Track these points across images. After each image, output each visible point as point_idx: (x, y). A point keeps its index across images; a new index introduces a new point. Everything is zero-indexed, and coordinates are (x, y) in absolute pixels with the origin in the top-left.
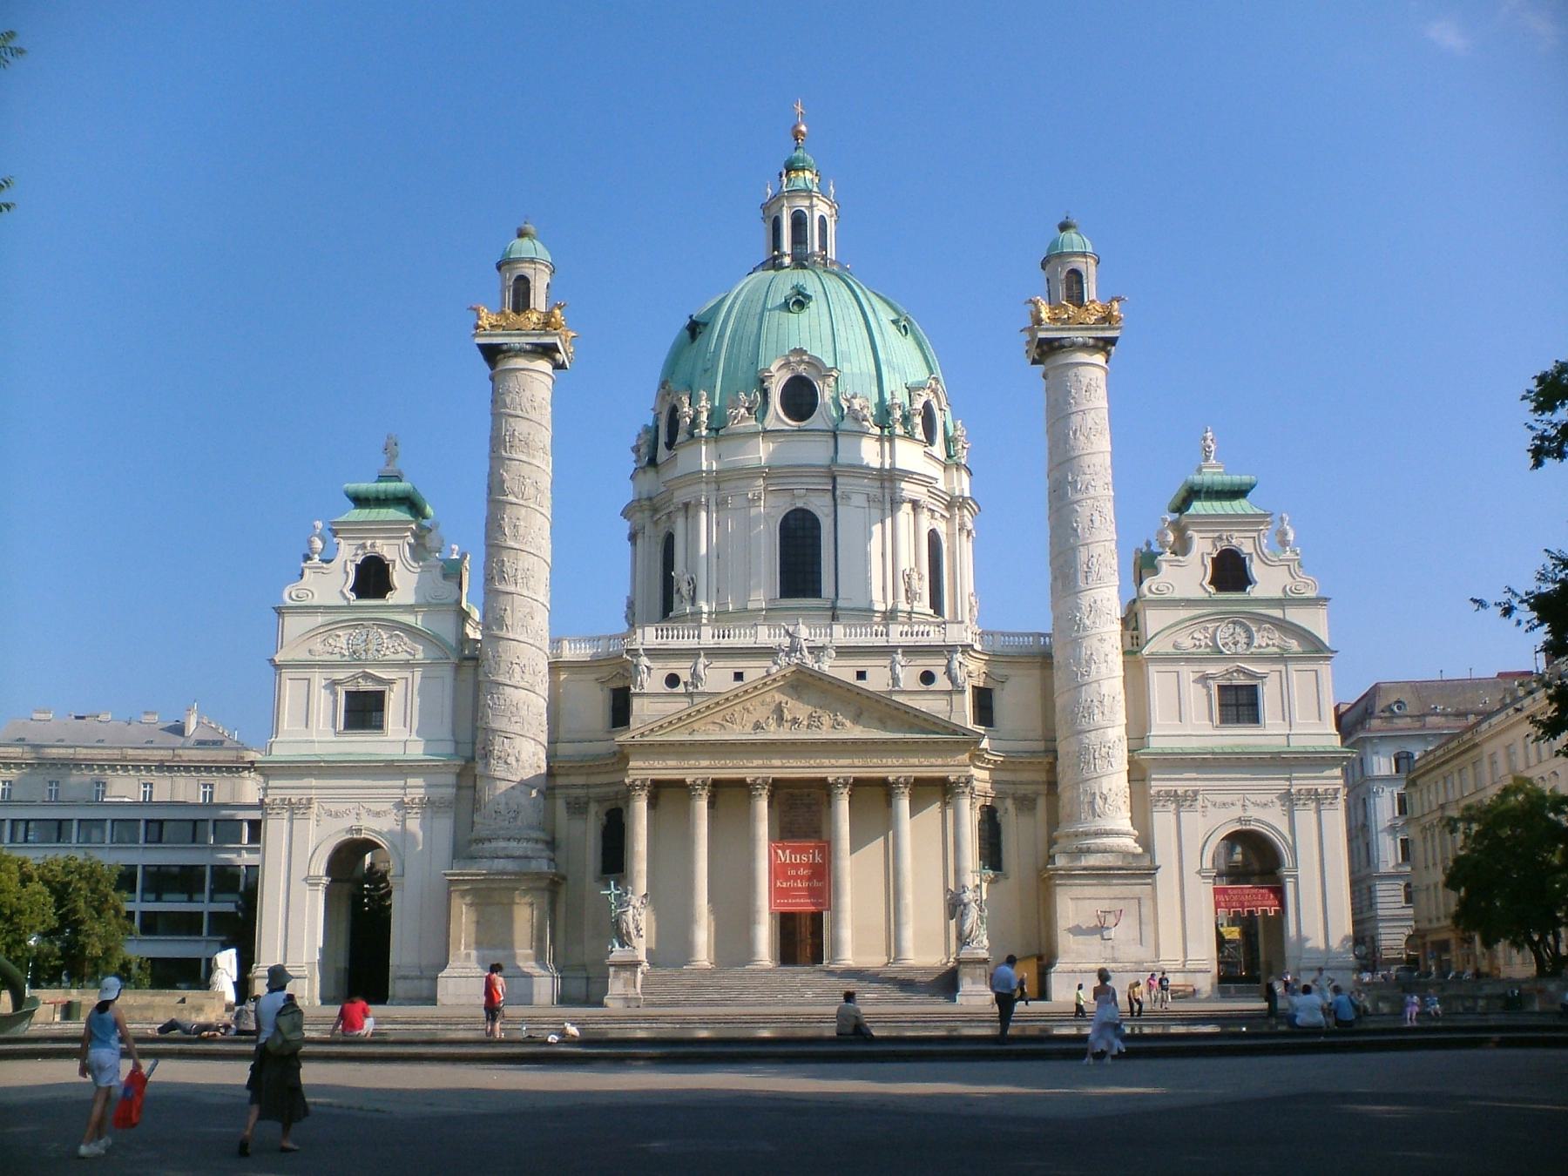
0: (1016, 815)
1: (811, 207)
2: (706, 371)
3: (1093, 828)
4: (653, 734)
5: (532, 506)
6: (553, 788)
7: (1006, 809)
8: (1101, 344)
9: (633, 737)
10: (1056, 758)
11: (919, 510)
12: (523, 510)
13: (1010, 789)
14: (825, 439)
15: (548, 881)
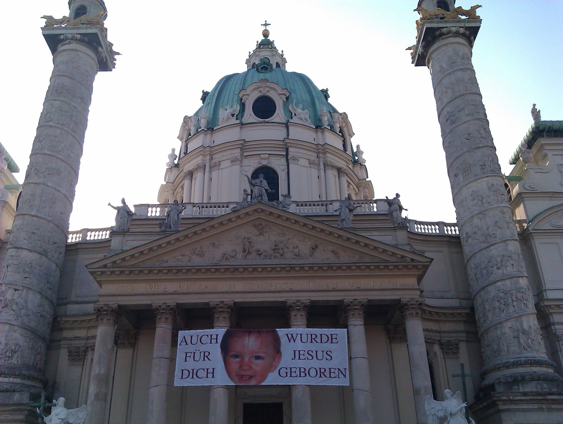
0: (444, 358)
1: (273, 55)
2: (209, 103)
3: (523, 359)
4: (124, 264)
5: (65, 129)
6: (60, 340)
7: (435, 353)
8: (468, 33)
9: (105, 266)
10: (472, 309)
11: (342, 174)
12: (59, 131)
13: (437, 337)
14: (281, 128)
15: (27, 412)
